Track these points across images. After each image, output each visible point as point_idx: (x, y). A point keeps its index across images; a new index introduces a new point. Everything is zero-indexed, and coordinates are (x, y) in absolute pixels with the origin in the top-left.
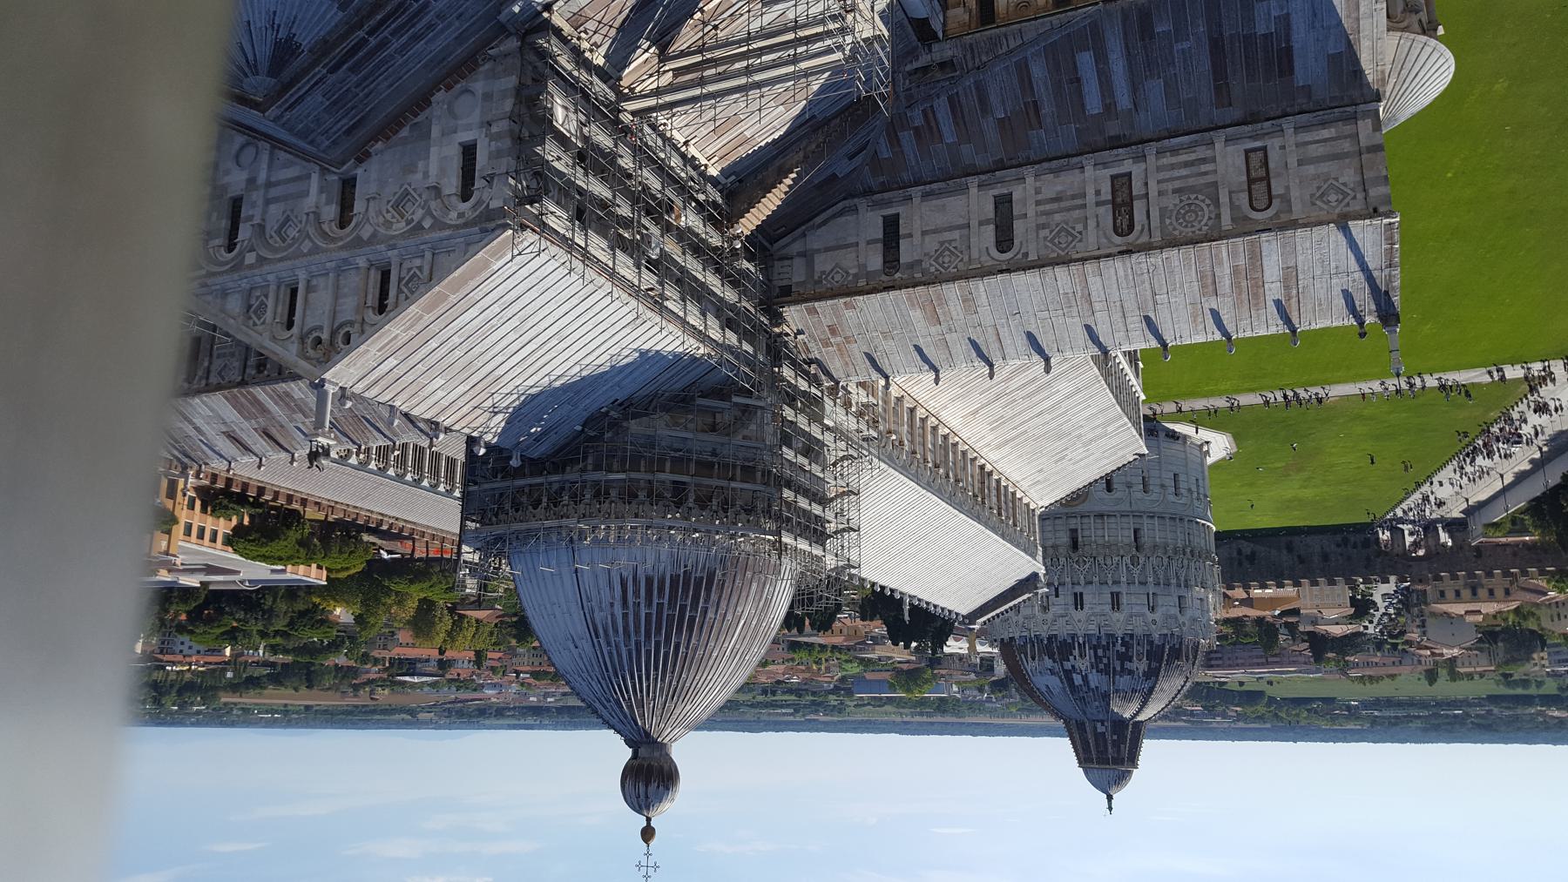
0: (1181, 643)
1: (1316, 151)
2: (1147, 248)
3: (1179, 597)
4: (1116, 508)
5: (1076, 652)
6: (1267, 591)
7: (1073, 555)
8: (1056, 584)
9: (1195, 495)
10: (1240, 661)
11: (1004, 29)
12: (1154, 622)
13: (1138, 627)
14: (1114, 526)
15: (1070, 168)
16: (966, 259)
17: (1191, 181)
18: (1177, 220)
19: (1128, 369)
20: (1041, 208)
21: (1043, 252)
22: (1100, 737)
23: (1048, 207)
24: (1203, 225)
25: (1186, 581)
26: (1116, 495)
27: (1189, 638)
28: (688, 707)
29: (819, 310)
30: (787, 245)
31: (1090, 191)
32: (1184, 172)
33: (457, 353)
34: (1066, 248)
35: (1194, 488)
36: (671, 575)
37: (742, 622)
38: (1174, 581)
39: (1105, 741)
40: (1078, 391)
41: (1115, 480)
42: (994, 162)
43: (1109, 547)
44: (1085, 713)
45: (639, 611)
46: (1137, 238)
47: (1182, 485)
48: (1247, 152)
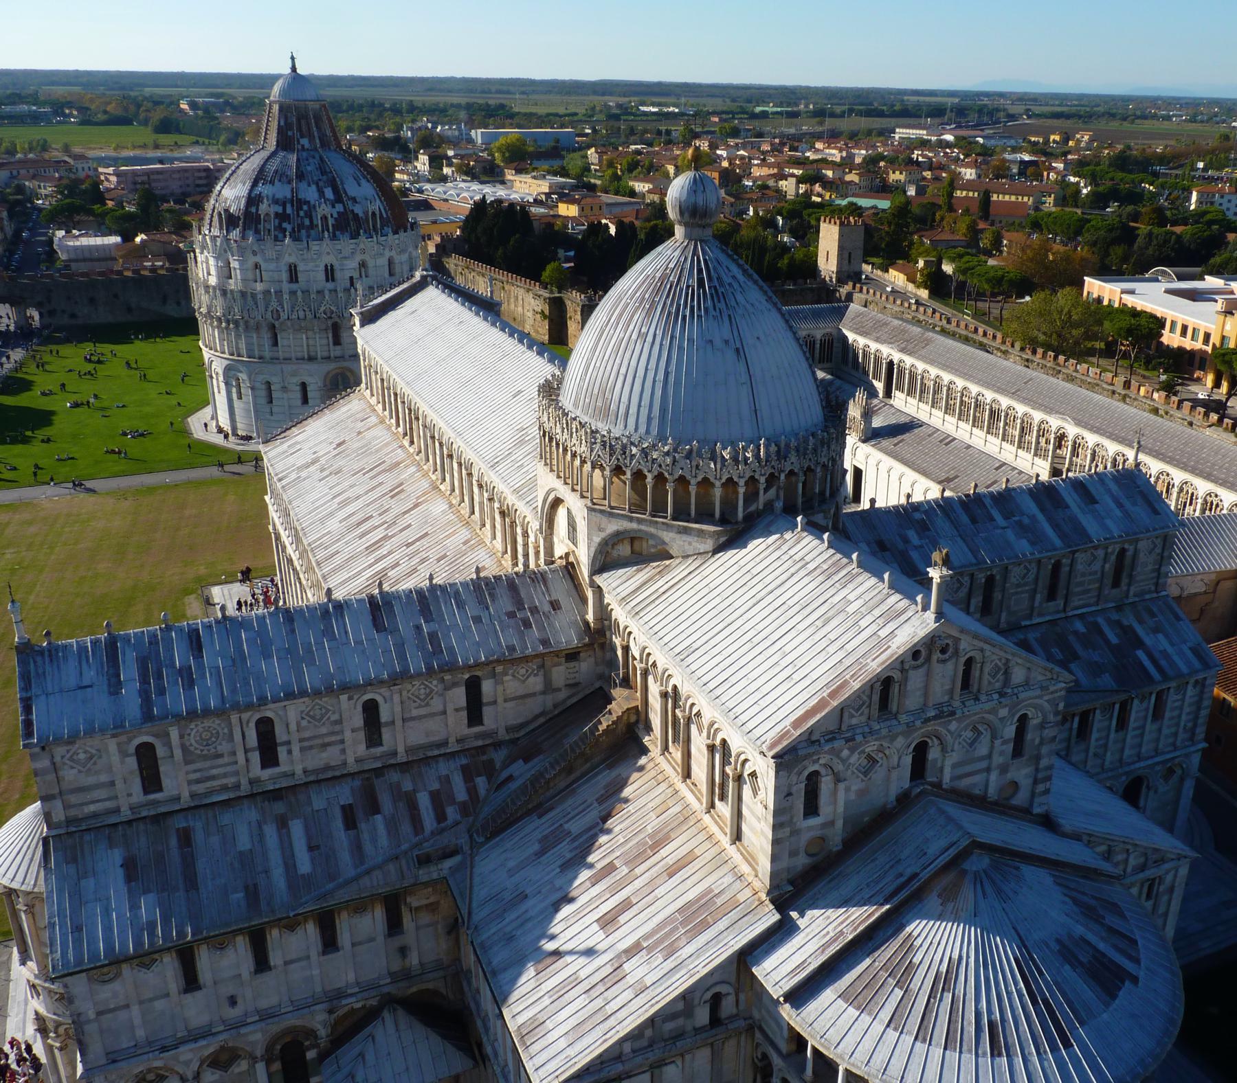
4: (295, 367)
5: (331, 222)
10: (176, 176)
12: (255, 253)
13: (270, 249)
14: (298, 349)
15: (316, 771)
16: (404, 693)
20: (338, 738)
23: (333, 738)
26: (296, 380)
30: (569, 697)
39: (300, 129)
40: (322, 521)
41: (299, 395)
42: (383, 775)
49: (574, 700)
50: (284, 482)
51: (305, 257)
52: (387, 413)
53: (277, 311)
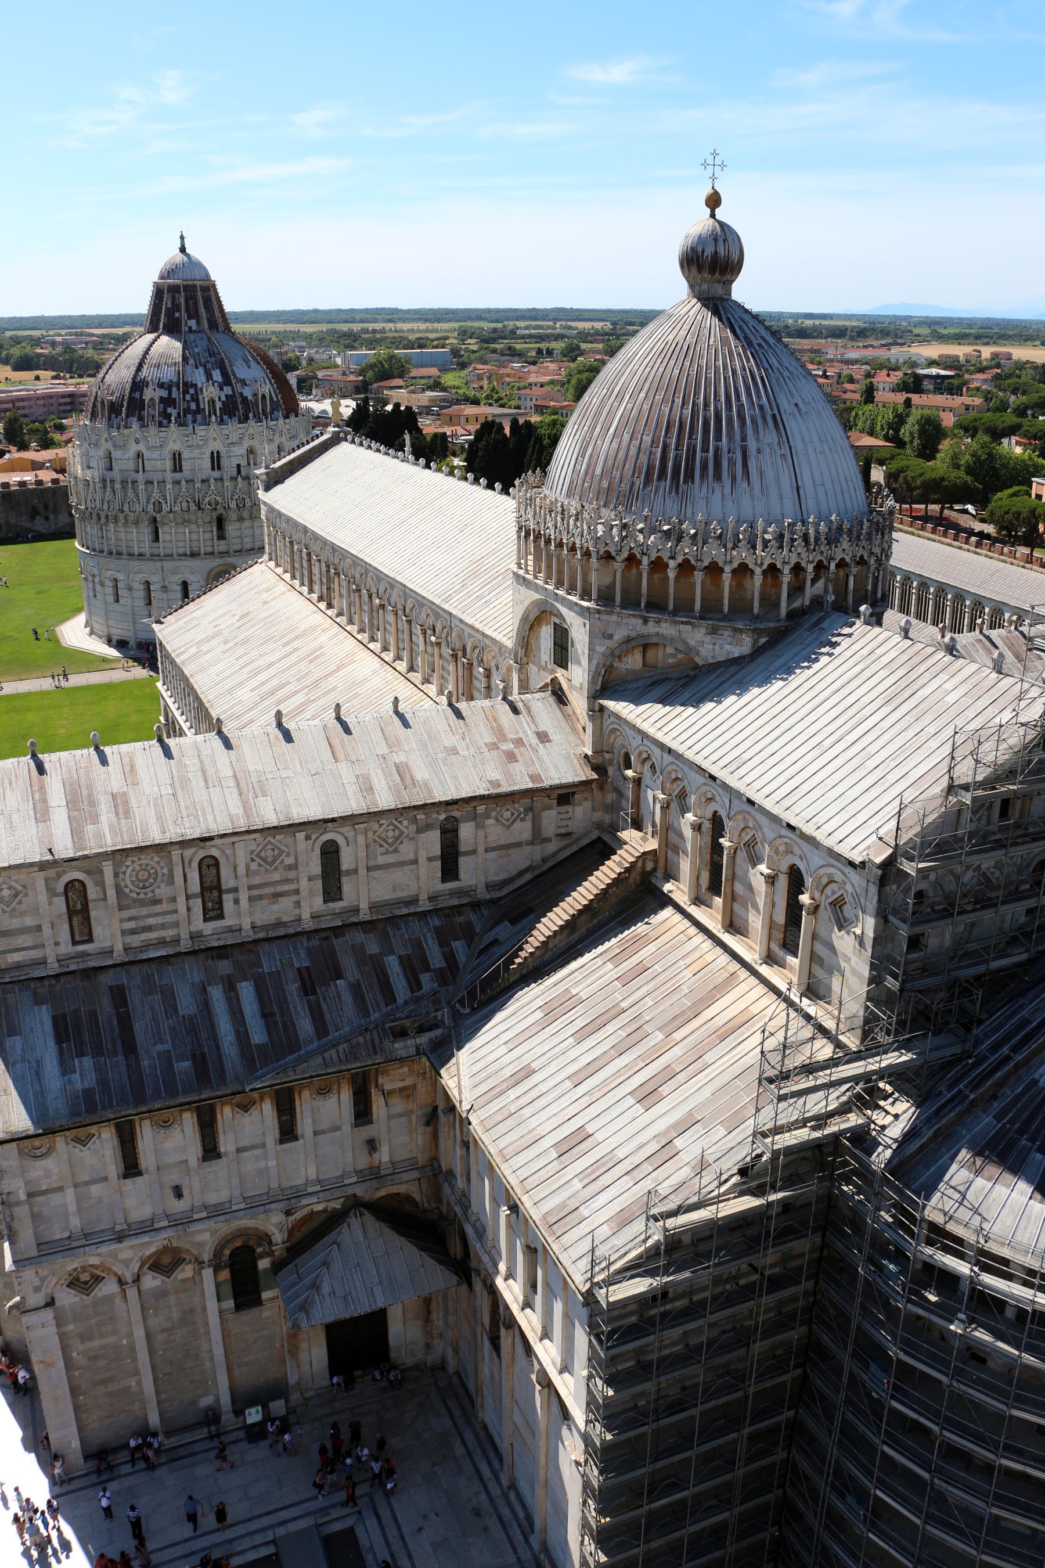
0: (110, 419)
1: (26, 940)
2: (184, 844)
3: (111, 469)
5: (218, 405)
6: (18, 479)
7: (222, 511)
8: (240, 479)
9: (97, 580)
10: (41, 402)
11: (343, 1068)
12: (137, 441)
14: (180, 544)
15: (263, 927)
16: (370, 834)
17: (144, 911)
18: (156, 873)
19: (177, 714)
20: (293, 887)
21: (289, 840)
22: (193, 314)
24: (131, 866)
25: (105, 487)
26: (178, 578)
27: (101, 425)
28: (671, 337)
29: (528, 779)
30: (560, 850)
31: (244, 903)
32: (151, 921)
33: (932, 730)
34: (266, 845)
35: (98, 587)
36: (693, 483)
37: (612, 430)
38: (118, 486)
39: (187, 310)
41: (179, 595)
42: (343, 935)
43: (185, 521)
44: (209, 339)
45: (729, 443)
46: (194, 854)
47: (110, 591)
48: (90, 940)
49: (567, 853)
50: (183, 657)
51: (190, 443)
52: (296, 583)
53: (160, 503)
